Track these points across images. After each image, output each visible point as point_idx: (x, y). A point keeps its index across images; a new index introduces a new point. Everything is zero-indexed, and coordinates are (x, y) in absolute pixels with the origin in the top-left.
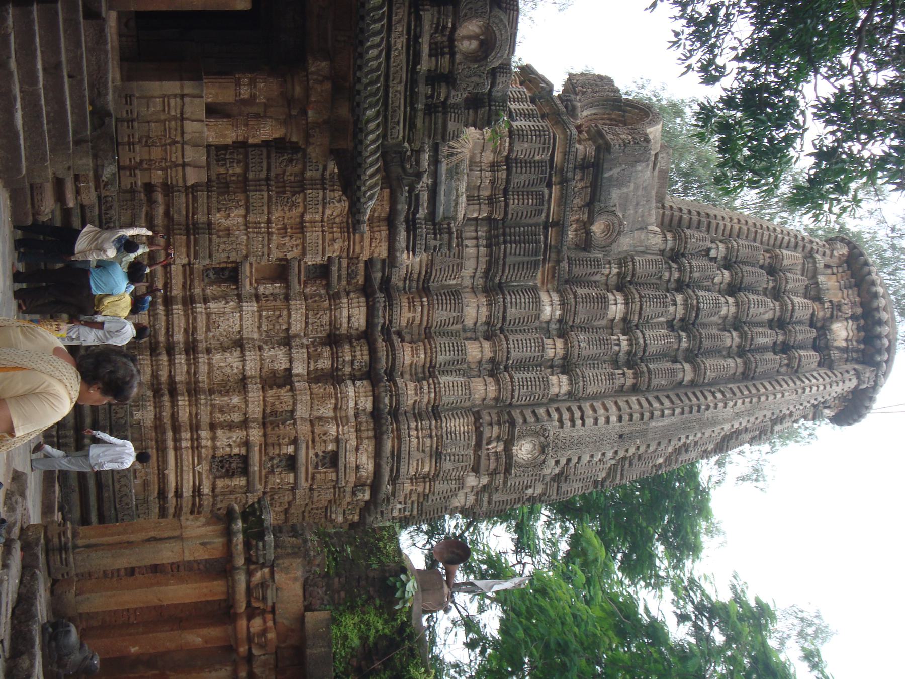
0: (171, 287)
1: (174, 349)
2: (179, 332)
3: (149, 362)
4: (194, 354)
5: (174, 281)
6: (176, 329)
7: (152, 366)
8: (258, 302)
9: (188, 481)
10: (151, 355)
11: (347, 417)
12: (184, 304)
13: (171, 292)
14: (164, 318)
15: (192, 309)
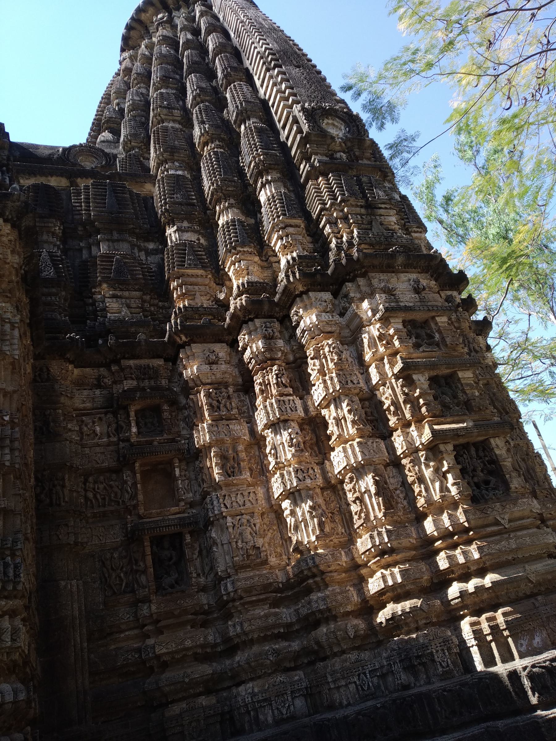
0: (202, 646)
1: (307, 617)
2: (276, 614)
3: (337, 659)
4: (308, 578)
5: (188, 643)
6: (271, 620)
7: (343, 652)
8: (208, 493)
9: (530, 535)
10: (324, 659)
11: (348, 326)
12: (229, 616)
13: (216, 645)
14: (256, 649)
15: (234, 600)
